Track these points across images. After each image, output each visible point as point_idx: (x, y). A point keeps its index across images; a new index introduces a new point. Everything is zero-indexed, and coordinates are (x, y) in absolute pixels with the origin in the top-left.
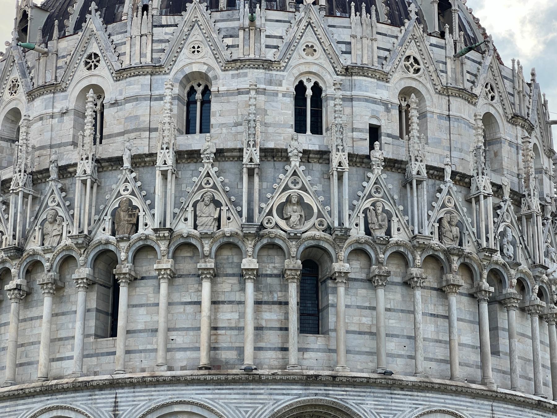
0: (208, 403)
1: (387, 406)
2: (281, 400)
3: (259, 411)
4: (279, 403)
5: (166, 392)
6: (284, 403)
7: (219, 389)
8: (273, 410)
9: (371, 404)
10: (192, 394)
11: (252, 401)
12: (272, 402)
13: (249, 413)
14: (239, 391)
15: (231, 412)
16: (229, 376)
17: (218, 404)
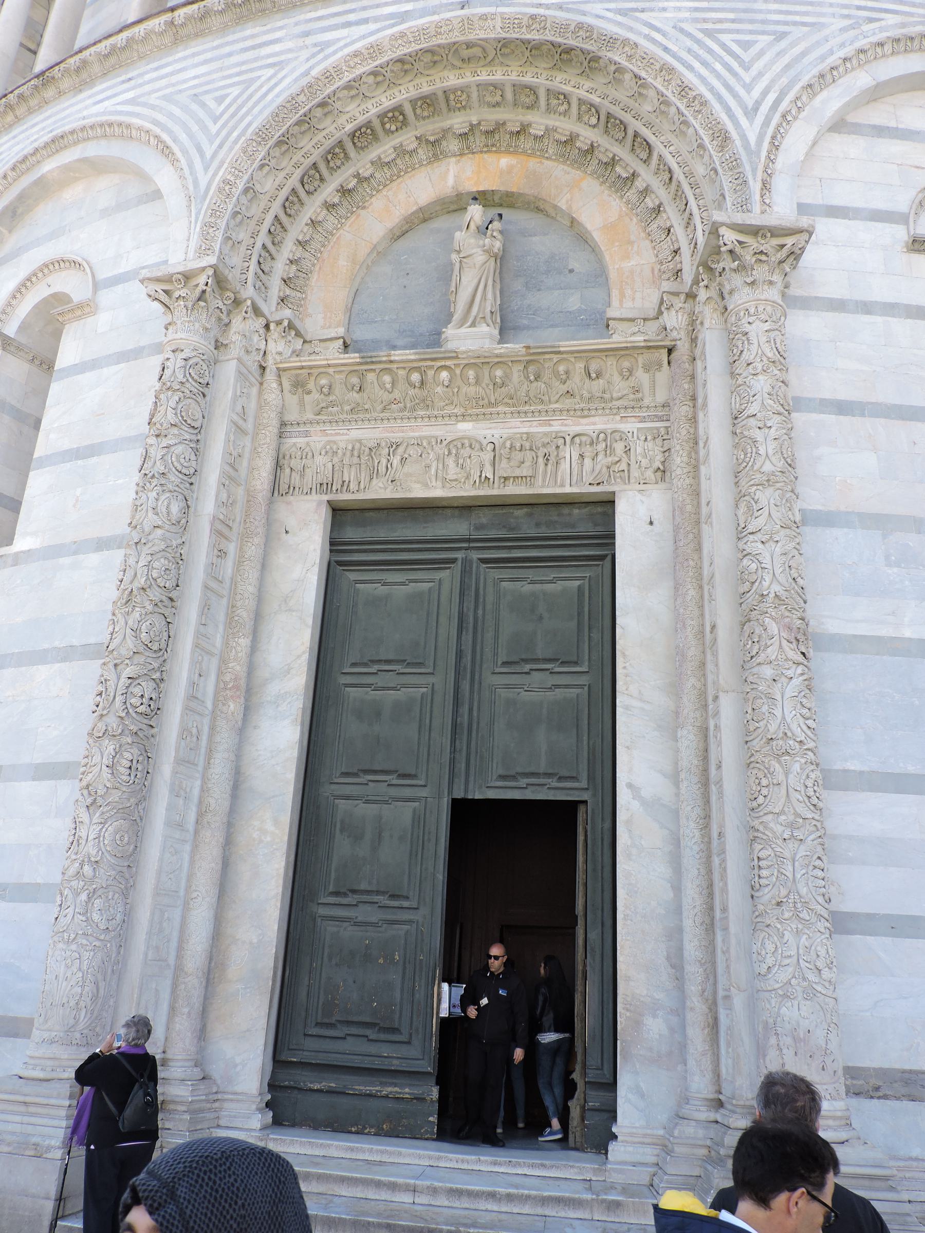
0: (120, 113)
1: (745, 11)
2: (339, 40)
3: (261, 86)
4: (331, 50)
5: (27, 133)
6: (346, 46)
7: (157, 69)
8: (307, 73)
9: (679, 9)
10: (86, 108)
11: (244, 68)
12: (305, 54)
13: (228, 101)
14: (209, 55)
15: (177, 112)
16: (176, 13)
17: (145, 105)
